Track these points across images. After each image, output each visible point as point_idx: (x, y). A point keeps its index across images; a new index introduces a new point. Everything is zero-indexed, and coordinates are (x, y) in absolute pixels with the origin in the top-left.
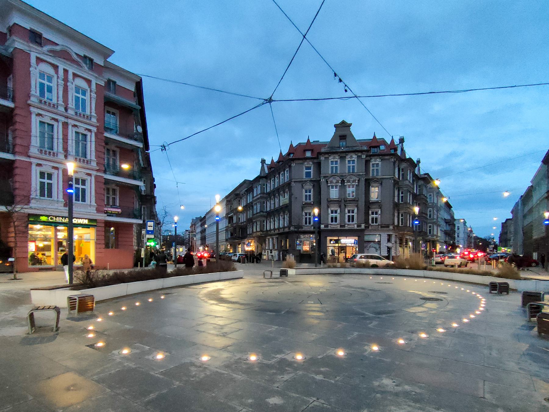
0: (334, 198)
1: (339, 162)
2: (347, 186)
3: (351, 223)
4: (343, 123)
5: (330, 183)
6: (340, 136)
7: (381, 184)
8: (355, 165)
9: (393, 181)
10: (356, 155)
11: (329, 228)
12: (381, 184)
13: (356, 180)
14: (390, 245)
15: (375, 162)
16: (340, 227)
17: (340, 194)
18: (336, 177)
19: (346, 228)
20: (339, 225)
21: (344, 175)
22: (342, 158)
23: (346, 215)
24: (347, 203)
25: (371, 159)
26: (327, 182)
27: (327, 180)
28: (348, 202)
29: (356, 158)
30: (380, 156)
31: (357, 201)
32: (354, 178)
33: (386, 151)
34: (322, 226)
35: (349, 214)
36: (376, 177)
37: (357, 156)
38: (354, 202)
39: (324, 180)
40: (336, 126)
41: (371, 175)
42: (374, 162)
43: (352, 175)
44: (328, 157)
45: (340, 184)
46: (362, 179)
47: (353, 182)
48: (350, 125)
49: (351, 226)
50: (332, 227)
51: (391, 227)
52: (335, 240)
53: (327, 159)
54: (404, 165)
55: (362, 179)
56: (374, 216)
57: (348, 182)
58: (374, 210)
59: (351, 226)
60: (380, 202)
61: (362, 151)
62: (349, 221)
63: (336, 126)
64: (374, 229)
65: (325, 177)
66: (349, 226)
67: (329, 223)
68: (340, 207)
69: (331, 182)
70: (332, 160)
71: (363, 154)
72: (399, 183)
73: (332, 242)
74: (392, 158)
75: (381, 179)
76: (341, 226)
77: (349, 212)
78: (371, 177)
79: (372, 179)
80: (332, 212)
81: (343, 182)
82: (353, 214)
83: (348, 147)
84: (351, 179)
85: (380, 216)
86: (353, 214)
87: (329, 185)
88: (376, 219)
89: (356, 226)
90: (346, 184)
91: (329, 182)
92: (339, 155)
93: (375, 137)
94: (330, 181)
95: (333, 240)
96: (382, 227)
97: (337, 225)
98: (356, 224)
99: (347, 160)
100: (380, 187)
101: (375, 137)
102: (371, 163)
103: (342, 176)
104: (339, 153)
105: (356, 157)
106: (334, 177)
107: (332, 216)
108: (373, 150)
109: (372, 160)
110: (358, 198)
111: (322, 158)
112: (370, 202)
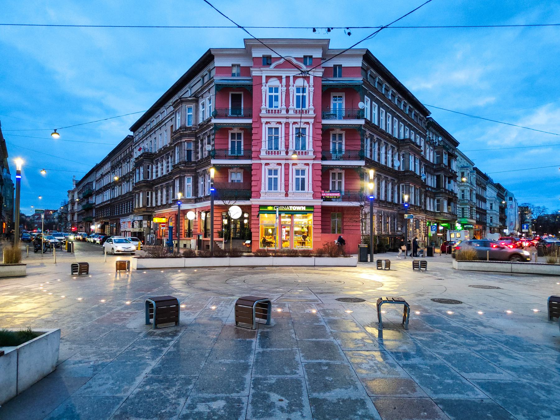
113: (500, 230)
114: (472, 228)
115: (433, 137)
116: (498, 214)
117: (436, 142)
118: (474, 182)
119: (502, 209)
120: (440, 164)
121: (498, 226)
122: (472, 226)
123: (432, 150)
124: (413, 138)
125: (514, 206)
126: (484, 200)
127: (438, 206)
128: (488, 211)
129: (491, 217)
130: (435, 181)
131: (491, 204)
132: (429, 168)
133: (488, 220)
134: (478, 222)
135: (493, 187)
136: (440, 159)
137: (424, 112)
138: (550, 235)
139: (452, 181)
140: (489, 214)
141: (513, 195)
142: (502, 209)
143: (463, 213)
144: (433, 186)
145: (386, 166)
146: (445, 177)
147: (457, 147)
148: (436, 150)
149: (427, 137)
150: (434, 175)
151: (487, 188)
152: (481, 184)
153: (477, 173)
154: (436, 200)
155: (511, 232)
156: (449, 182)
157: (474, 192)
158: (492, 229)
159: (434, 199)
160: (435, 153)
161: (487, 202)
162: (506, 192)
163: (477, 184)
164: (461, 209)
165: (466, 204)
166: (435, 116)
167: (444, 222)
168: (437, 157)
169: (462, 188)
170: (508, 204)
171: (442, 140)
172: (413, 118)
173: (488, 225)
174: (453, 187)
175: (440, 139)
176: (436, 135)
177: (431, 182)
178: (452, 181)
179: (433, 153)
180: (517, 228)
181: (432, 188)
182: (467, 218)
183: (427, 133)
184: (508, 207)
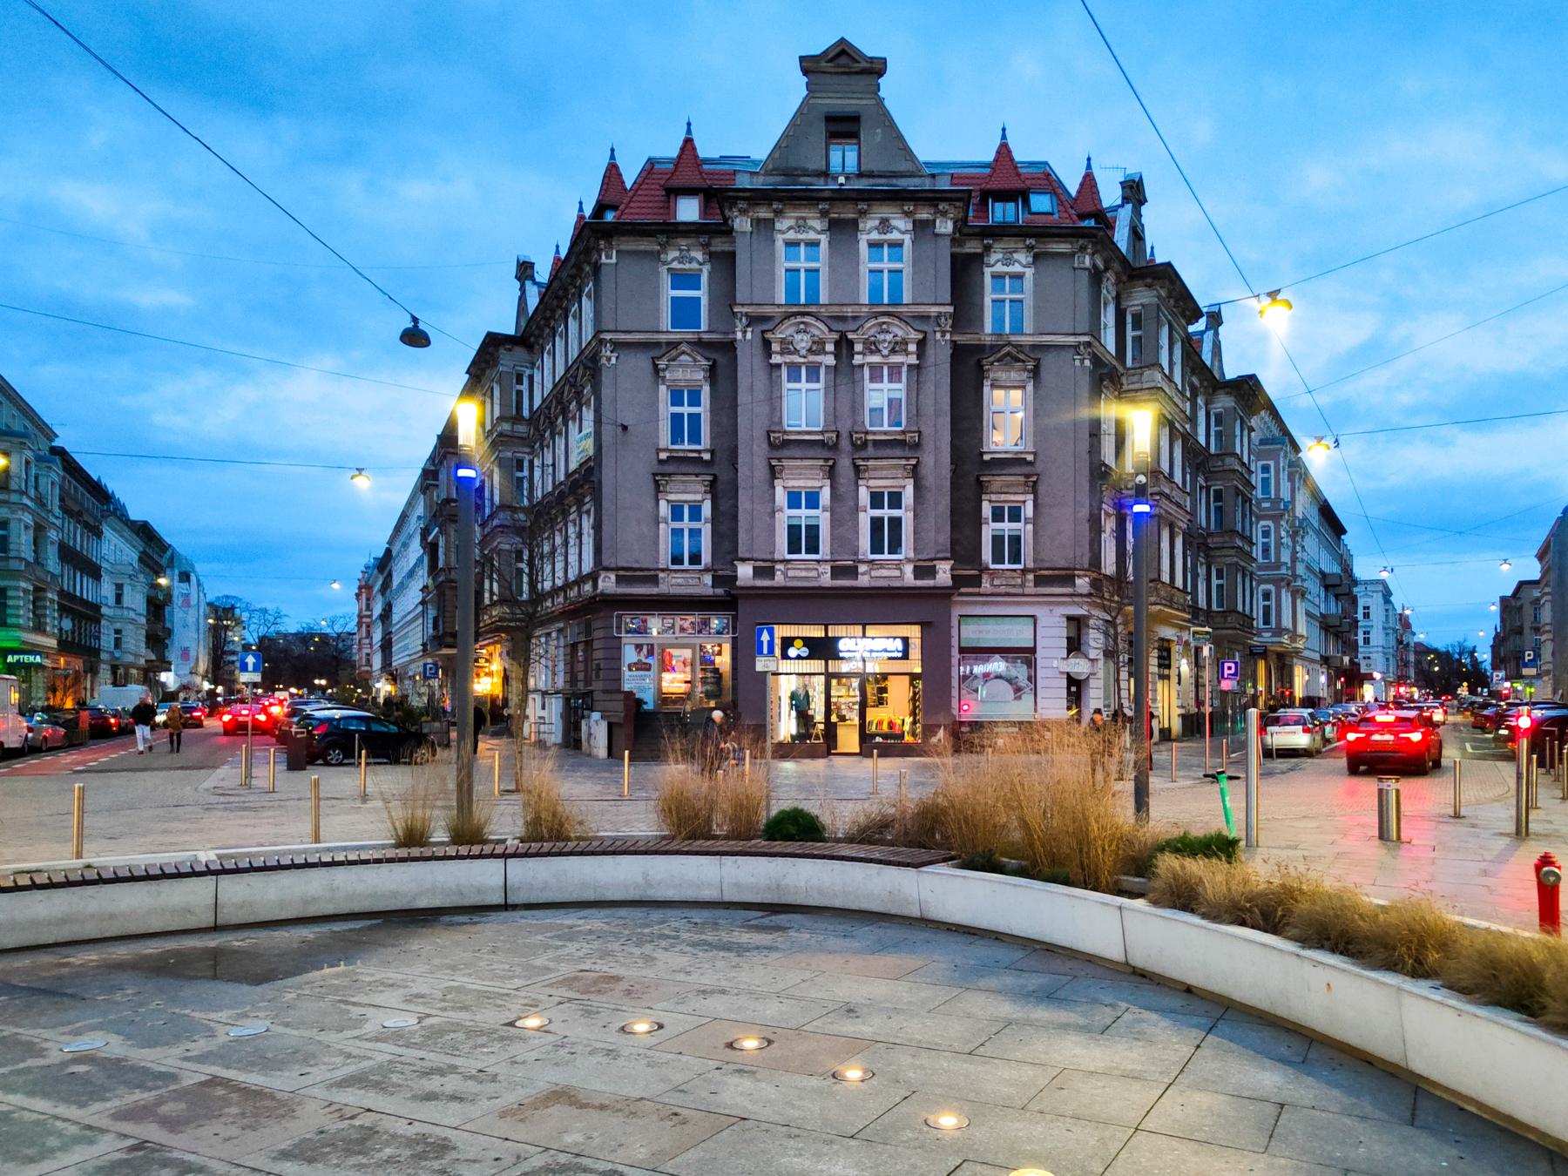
0: (804, 428)
1: (824, 245)
2: (866, 371)
3: (886, 556)
4: (843, 53)
5: (782, 353)
6: (830, 119)
7: (1036, 373)
8: (906, 265)
9: (1087, 363)
10: (907, 214)
11: (779, 580)
12: (1036, 373)
13: (905, 342)
14: (1079, 667)
15: (1006, 269)
16: (833, 577)
17: (833, 414)
18: (807, 319)
19: (863, 581)
20: (828, 568)
21: (849, 311)
22: (842, 230)
23: (861, 515)
24: (863, 454)
25: (988, 248)
26: (767, 344)
27: (763, 332)
28: (870, 451)
30: (1030, 236)
31: (917, 446)
32: (899, 331)
33: (1056, 217)
34: (745, 572)
35: (877, 513)
36: (1012, 338)
37: (914, 222)
38: (898, 452)
39: (749, 336)
40: (809, 65)
41: (988, 328)
42: (999, 268)
44: (772, 222)
45: (830, 360)
47: (893, 351)
48: (877, 68)
49: (884, 573)
50: (791, 573)
51: (1082, 584)
52: (808, 642)
53: (765, 227)
54: (1141, 298)
55: (938, 335)
56: (1007, 527)
57: (872, 352)
58: (1003, 497)
59: (884, 573)
60: (1030, 458)
61: (933, 198)
62: (877, 547)
63: (809, 65)
64: (1003, 589)
65: (753, 320)
66: (874, 573)
67: (777, 556)
68: (832, 473)
69: (787, 347)
70: (791, 235)
71: (944, 214)
72: (1124, 380)
73: (792, 652)
74: (1083, 249)
75: (1035, 347)
76: (837, 572)
77: (876, 500)
78: (988, 340)
79: (995, 348)
80: (794, 501)
81: (844, 346)
82: (895, 513)
84: (881, 337)
85: (1030, 527)
86: (895, 513)
87: (776, 359)
88: (1016, 540)
89: (909, 569)
90: (858, 360)
91: (775, 347)
92: (824, 214)
93: (1004, 151)
94: (783, 341)
95: (798, 643)
96: (1039, 581)
97: (815, 565)
98: (909, 560)
99: (863, 240)
100: (1030, 387)
101: (1004, 151)
102: (988, 271)
103: (842, 319)
104: (824, 199)
105: (910, 226)
106: (799, 319)
107: (795, 522)
108: (1002, 212)
109: (994, 257)
110: (920, 432)
111: (742, 224)
112: (986, 457)
116: (143, 620)
119: (157, 606)
125: (194, 601)
128: (104, 610)
129: (118, 632)
133: (107, 641)
134: (66, 646)
140: (111, 619)
142: (157, 606)
182: (18, 626)
184: (177, 601)
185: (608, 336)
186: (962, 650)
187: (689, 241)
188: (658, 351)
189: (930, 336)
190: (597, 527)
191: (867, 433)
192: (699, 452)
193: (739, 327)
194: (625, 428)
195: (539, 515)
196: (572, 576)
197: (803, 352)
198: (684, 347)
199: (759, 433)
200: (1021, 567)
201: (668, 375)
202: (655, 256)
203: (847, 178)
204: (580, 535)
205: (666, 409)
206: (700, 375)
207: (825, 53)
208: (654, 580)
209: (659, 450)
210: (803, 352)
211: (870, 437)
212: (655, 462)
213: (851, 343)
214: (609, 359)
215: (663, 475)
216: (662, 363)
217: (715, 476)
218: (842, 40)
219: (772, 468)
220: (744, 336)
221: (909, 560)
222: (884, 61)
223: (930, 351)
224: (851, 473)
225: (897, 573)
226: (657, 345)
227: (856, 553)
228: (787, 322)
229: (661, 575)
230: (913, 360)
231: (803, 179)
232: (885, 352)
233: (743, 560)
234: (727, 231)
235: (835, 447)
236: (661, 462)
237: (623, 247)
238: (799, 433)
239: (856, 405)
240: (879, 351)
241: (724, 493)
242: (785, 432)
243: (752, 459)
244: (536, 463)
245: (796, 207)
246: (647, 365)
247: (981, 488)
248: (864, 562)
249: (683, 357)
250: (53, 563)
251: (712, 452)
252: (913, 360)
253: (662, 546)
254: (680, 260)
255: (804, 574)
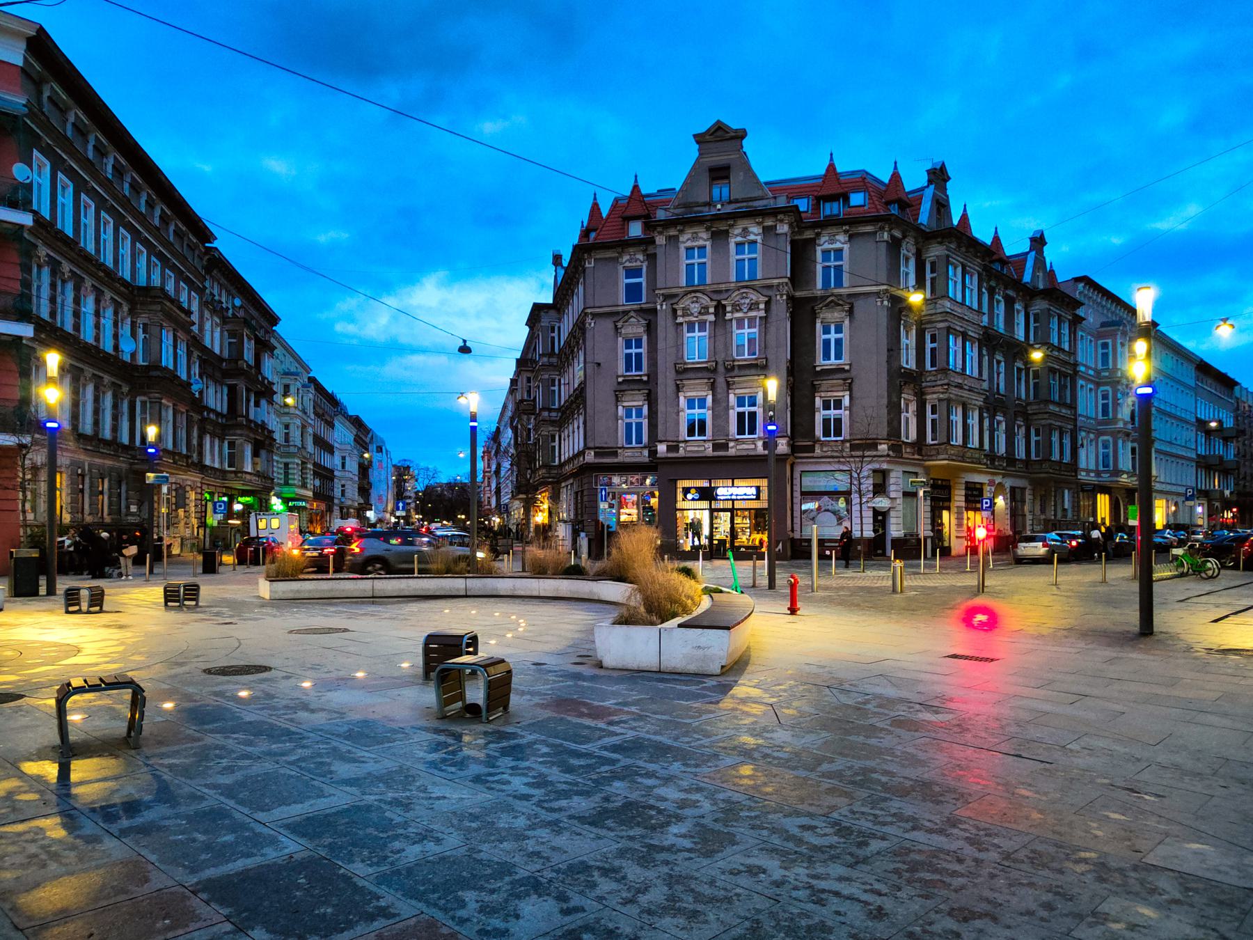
0: (697, 360)
1: (708, 249)
2: (734, 323)
3: (747, 436)
5: (683, 316)
8: (758, 255)
10: (758, 223)
11: (682, 452)
13: (757, 303)
14: (882, 503)
16: (714, 450)
17: (714, 351)
18: (698, 295)
19: (732, 452)
20: (710, 445)
21: (723, 287)
22: (720, 237)
23: (731, 411)
24: (733, 374)
26: (675, 311)
28: (736, 372)
29: (759, 234)
32: (754, 296)
34: (662, 448)
35: (741, 409)
37: (764, 228)
39: (664, 307)
40: (699, 139)
43: (746, 287)
45: (712, 318)
46: (778, 297)
47: (750, 309)
48: (741, 135)
49: (745, 446)
50: (688, 449)
51: (883, 447)
52: (698, 489)
53: (673, 240)
55: (778, 297)
56: (832, 413)
57: (737, 311)
58: (829, 394)
59: (745, 446)
60: (847, 367)
61: (774, 212)
62: (741, 431)
63: (699, 139)
64: (829, 454)
65: (667, 297)
66: (738, 447)
67: (681, 439)
68: (713, 387)
69: (686, 312)
70: (689, 244)
71: (781, 221)
73: (689, 496)
76: (716, 447)
77: (741, 402)
80: (691, 404)
81: (720, 309)
82: (753, 409)
83: (737, 201)
84: (743, 301)
85: (847, 412)
86: (753, 409)
87: (680, 320)
88: (838, 421)
89: (760, 444)
90: (728, 316)
91: (680, 313)
92: (708, 229)
94: (683, 309)
95: (693, 491)
96: (853, 448)
97: (702, 443)
98: (760, 438)
99: (732, 242)
103: (719, 292)
104: (707, 221)
105: (761, 231)
106: (693, 295)
107: (691, 417)
110: (766, 359)
111: (660, 240)
113: (360, 513)
114: (304, 508)
115: (220, 295)
117: (228, 309)
118: (310, 411)
120: (236, 361)
121: (356, 504)
122: (304, 504)
123: (217, 324)
124: (170, 287)
126: (330, 449)
127: (231, 456)
128: (336, 473)
129: (343, 486)
130: (225, 398)
131: (344, 458)
132: (211, 365)
133: (337, 492)
135: (348, 423)
136: (237, 349)
137: (201, 232)
138: (445, 522)
139: (263, 402)
140: (340, 479)
141: (383, 442)
143: (286, 474)
144: (219, 409)
145: (97, 348)
146: (248, 390)
147: (274, 328)
148: (227, 327)
149: (208, 291)
150: (222, 384)
151: (336, 423)
152: (323, 415)
153: (315, 389)
154: (226, 443)
155: (380, 516)
156: (257, 404)
157: (310, 430)
158: (345, 510)
159: (222, 440)
160: (226, 333)
161: (337, 453)
162: (370, 436)
163: (316, 414)
164: (282, 466)
165: (293, 455)
166: (224, 245)
167: (244, 493)
168: (230, 343)
169: (286, 419)
170: (374, 460)
171: (241, 307)
172: (171, 238)
173: (336, 501)
174: (264, 414)
175: (238, 302)
176: (229, 293)
177: (215, 399)
178: (263, 402)
179: (222, 332)
180: (390, 507)
181: (218, 414)
183: (207, 284)
185: (589, 311)
186: (803, 493)
187: (635, 249)
188: (618, 316)
189: (774, 298)
190: (585, 423)
191: (734, 361)
192: (640, 376)
193: (659, 302)
194: (599, 364)
195: (564, 413)
196: (576, 452)
197: (696, 314)
198: (632, 314)
199: (670, 365)
200: (841, 438)
201: (623, 331)
202: (615, 260)
203: (722, 205)
204: (578, 428)
205: (622, 351)
206: (641, 330)
207: (708, 130)
208: (615, 454)
209: (618, 376)
210: (696, 314)
211: (736, 363)
212: (615, 384)
213: (724, 307)
214: (590, 324)
215: (620, 391)
216: (619, 324)
217: (650, 390)
218: (718, 122)
219: (677, 386)
220: (663, 307)
221: (760, 438)
222: (744, 131)
223: (773, 307)
224: (724, 385)
225: (753, 446)
226: (617, 313)
227: (728, 435)
228: (685, 298)
229: (619, 451)
230: (762, 314)
231: (696, 209)
232: (745, 310)
233: (661, 442)
234: (652, 241)
235: (715, 371)
236: (619, 383)
237: (598, 257)
238: (693, 363)
239: (728, 346)
240: (741, 310)
241: (651, 399)
242: (685, 363)
243: (666, 379)
244: (562, 382)
245: (691, 227)
246: (611, 326)
247: (814, 389)
248: (731, 440)
249: (632, 320)
250: (310, 447)
251: (648, 376)
252: (762, 314)
253: (619, 434)
254: (630, 261)
255: (696, 449)
